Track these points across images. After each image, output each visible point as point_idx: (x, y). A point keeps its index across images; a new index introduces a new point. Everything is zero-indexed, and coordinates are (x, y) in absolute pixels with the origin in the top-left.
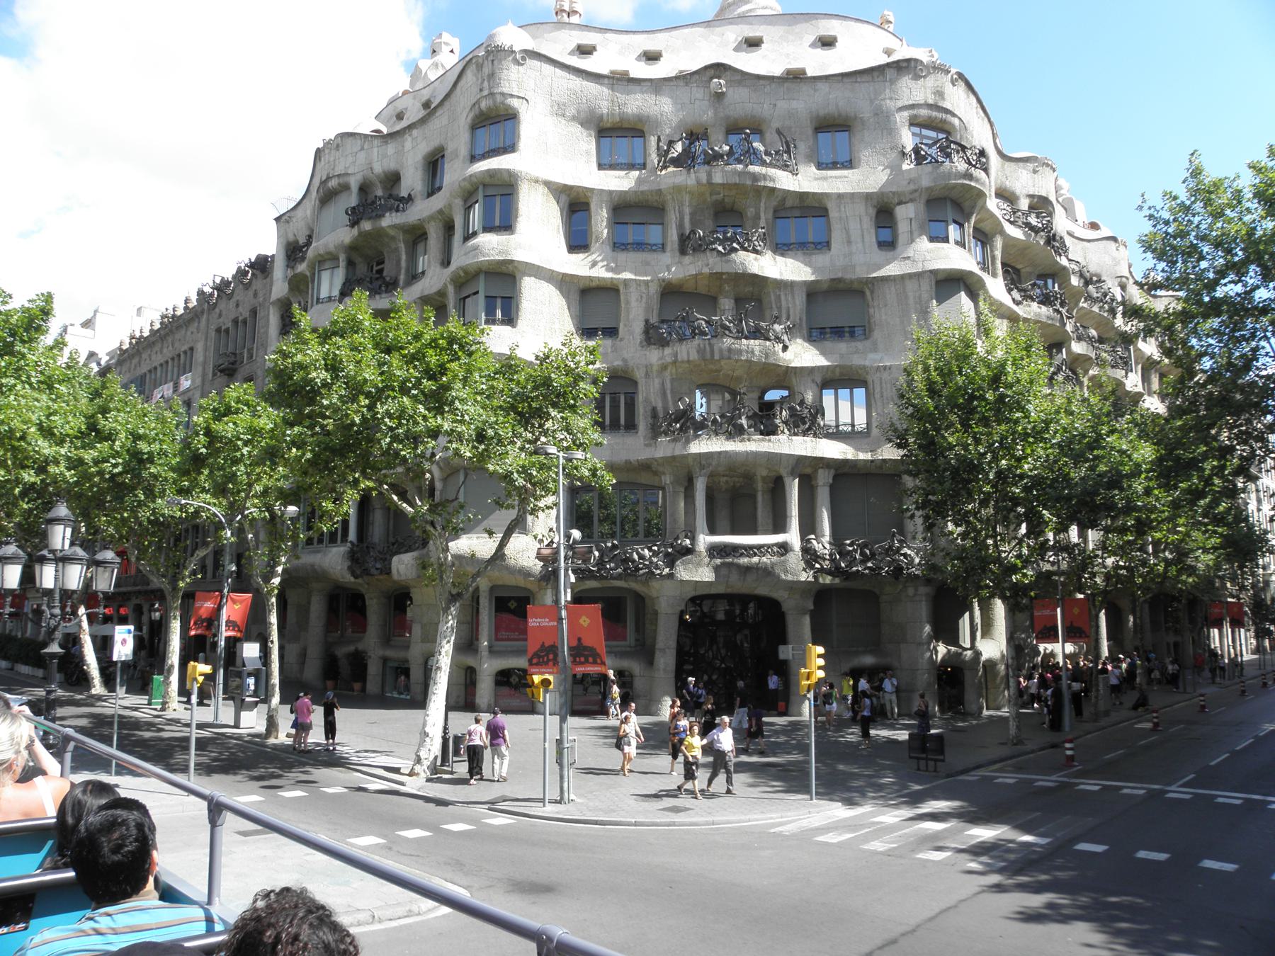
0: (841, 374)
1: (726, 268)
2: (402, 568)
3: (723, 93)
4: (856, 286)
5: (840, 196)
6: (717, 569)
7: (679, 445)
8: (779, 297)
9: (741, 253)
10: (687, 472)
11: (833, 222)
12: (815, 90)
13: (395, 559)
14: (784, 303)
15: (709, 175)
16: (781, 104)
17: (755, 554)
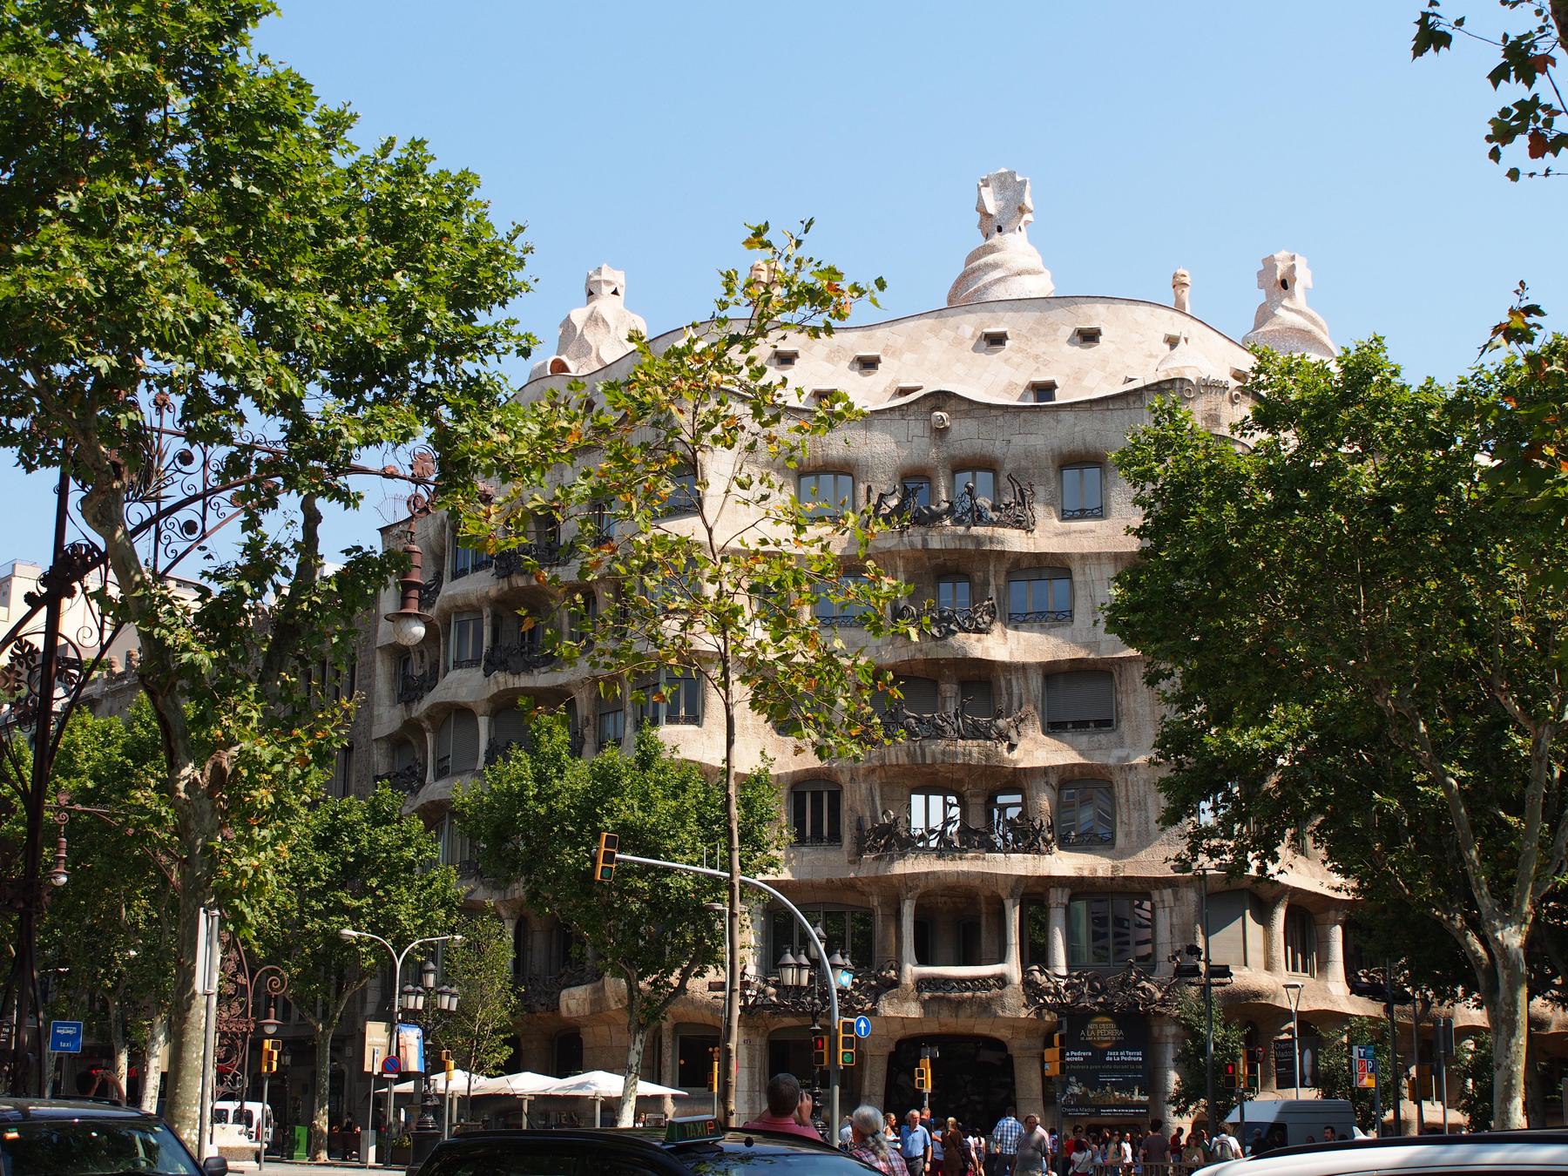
0: (1081, 773)
1: (942, 654)
2: (573, 1004)
3: (947, 428)
4: (1100, 666)
5: (1083, 557)
6: (925, 1004)
7: (883, 864)
8: (1009, 682)
9: (961, 636)
10: (894, 891)
11: (1077, 586)
12: (1058, 422)
13: (564, 993)
14: (1016, 691)
15: (925, 541)
16: (1018, 441)
17: (968, 989)
